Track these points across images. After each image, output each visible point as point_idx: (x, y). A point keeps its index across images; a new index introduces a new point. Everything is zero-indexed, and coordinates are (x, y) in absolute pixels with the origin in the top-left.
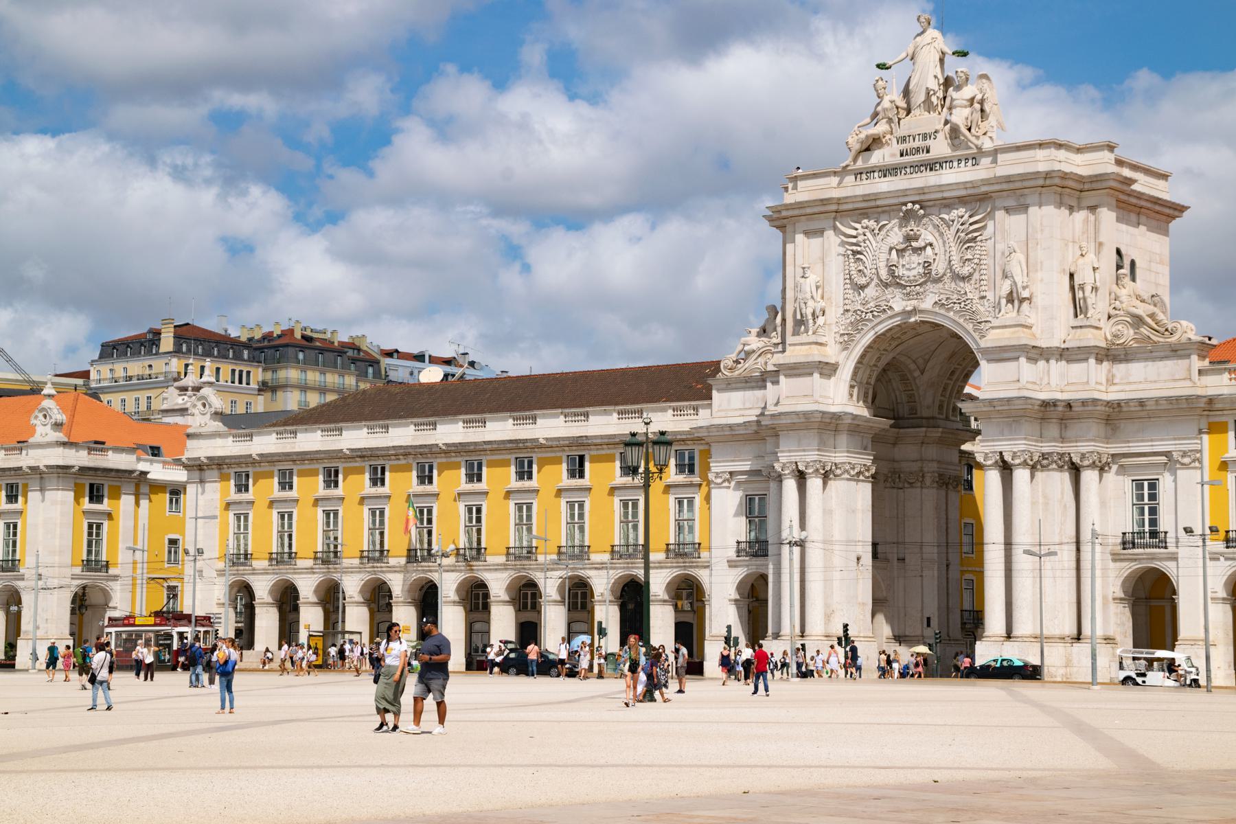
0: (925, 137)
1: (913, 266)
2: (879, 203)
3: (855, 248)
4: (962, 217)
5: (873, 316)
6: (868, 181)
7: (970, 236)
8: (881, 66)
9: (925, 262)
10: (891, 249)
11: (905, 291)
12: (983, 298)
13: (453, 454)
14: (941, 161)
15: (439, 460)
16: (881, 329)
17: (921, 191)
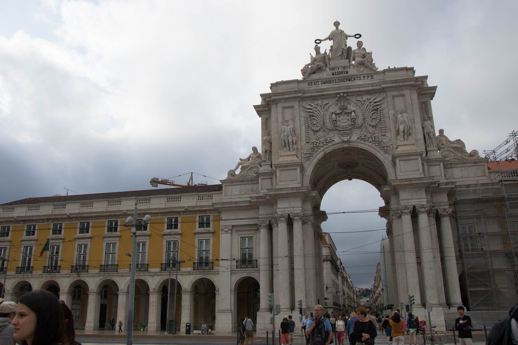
0: (344, 67)
1: (345, 121)
2: (325, 93)
3: (312, 114)
4: (370, 99)
5: (323, 144)
6: (316, 86)
7: (375, 107)
8: (318, 41)
9: (353, 118)
10: (333, 113)
11: (340, 133)
12: (385, 135)
13: (74, 219)
14: (354, 77)
15: (66, 222)
16: (328, 150)
17: (349, 87)
